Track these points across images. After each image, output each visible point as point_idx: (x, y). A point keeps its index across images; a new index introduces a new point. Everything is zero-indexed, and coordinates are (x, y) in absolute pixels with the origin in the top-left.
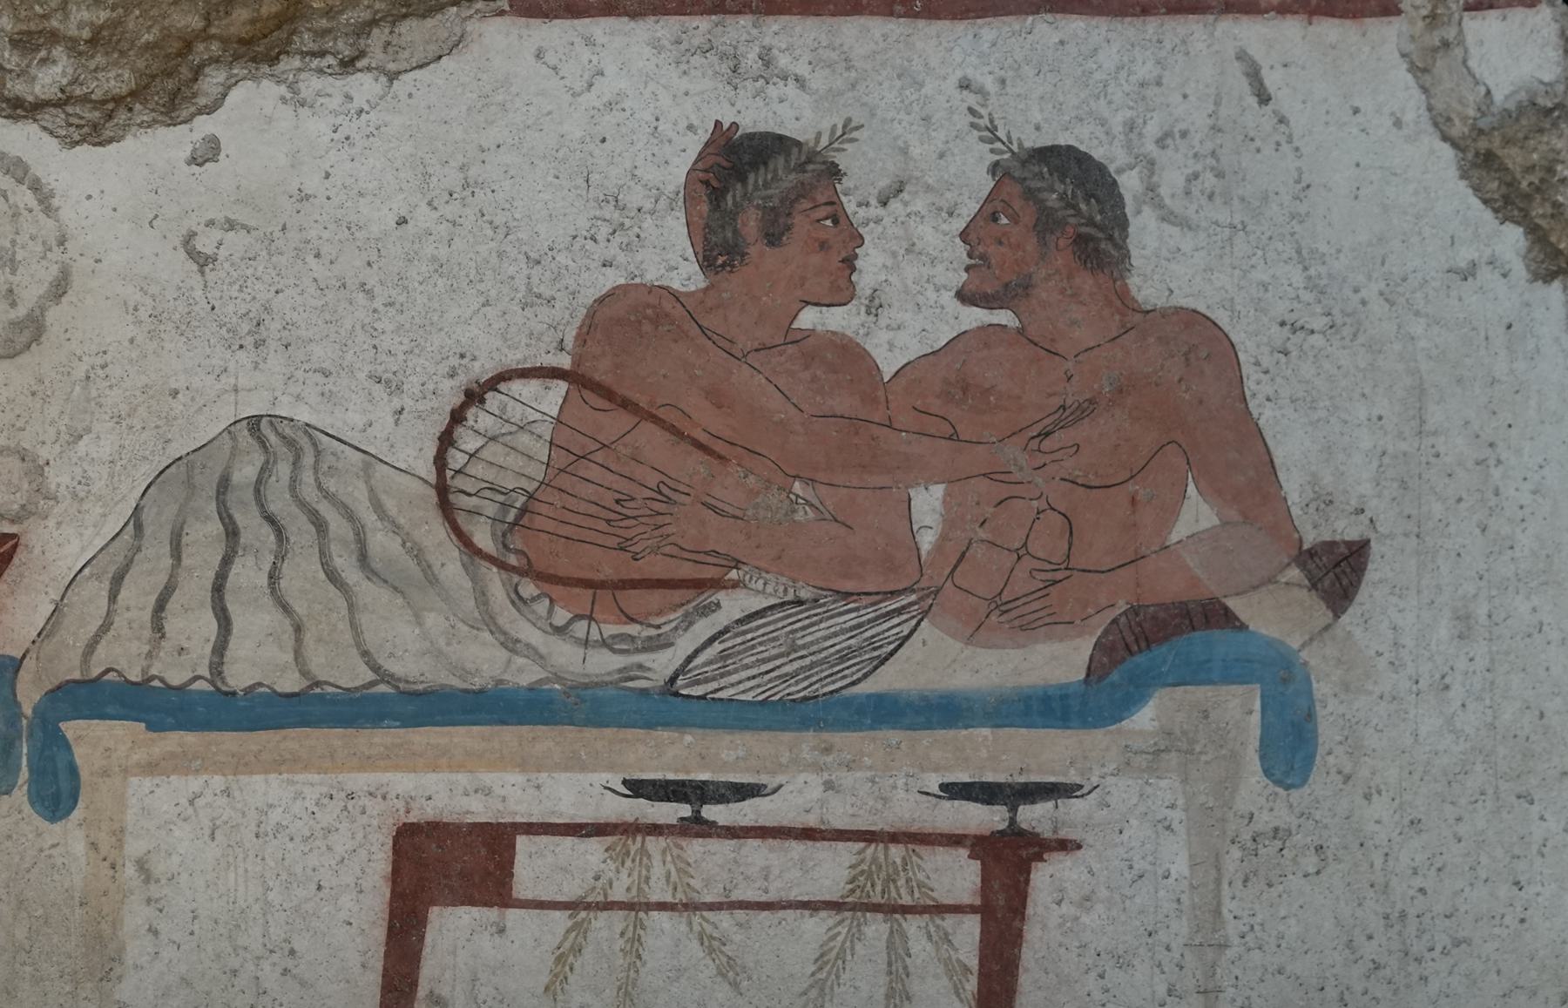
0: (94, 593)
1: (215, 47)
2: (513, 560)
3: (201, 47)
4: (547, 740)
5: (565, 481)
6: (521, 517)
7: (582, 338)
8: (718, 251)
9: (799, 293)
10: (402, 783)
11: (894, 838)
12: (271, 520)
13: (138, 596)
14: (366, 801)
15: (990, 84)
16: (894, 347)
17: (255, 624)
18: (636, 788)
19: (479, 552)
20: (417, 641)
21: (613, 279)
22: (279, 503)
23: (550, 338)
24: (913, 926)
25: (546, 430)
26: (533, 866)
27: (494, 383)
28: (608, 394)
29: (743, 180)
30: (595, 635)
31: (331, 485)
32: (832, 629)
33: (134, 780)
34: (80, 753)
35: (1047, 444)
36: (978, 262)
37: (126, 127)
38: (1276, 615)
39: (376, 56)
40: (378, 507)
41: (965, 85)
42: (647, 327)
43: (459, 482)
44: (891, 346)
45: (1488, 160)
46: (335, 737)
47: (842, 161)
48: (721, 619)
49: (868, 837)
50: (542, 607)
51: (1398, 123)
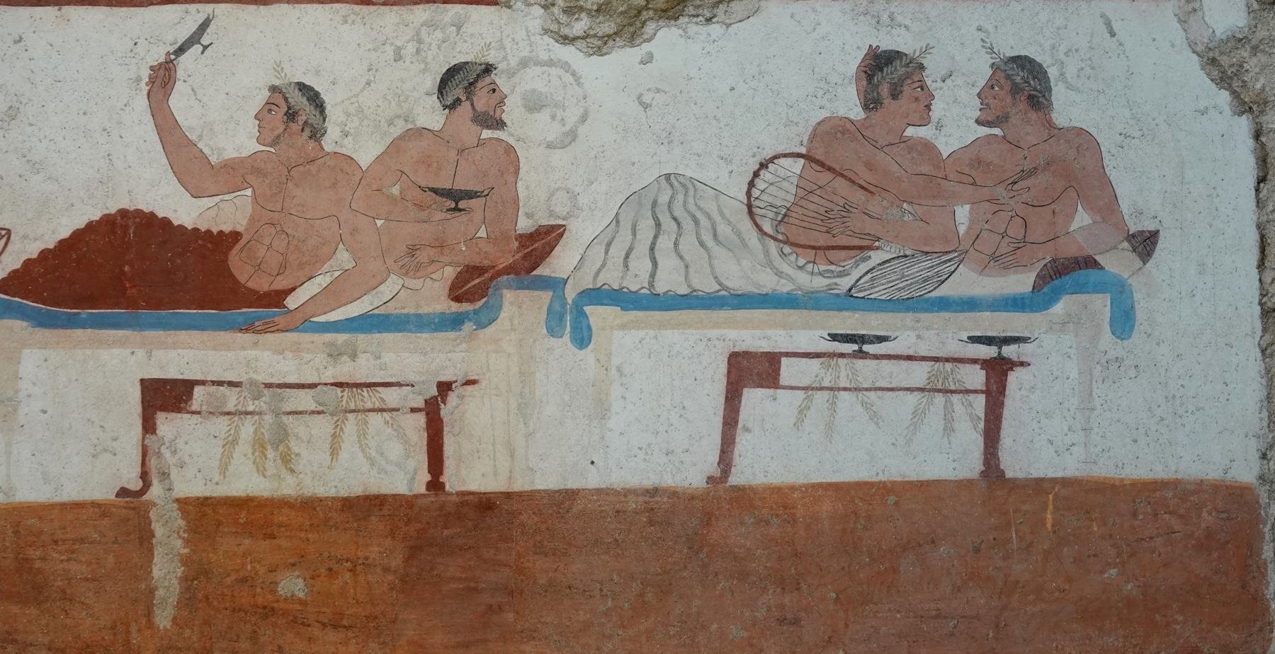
1: (651, 13)
2: (780, 237)
3: (645, 13)
4: (794, 315)
5: (803, 202)
7: (811, 140)
8: (871, 103)
9: (906, 121)
10: (732, 334)
11: (947, 360)
12: (675, 219)
13: (617, 252)
14: (717, 342)
15: (990, 28)
16: (948, 143)
17: (668, 263)
18: (834, 337)
19: (765, 234)
20: (740, 273)
21: (824, 114)
22: (679, 212)
23: (797, 140)
24: (955, 398)
25: (795, 180)
26: (790, 371)
27: (773, 159)
28: (822, 165)
29: (882, 71)
30: (816, 270)
31: (702, 204)
32: (921, 268)
33: (615, 332)
34: (592, 321)
35: (1016, 187)
36: (985, 107)
37: (613, 48)
38: (1118, 262)
39: (721, 15)
40: (721, 213)
41: (979, 29)
42: (839, 135)
43: (757, 203)
44: (947, 144)
45: (1213, 61)
46: (702, 314)
47: (925, 63)
48: (871, 264)
49: (936, 359)
50: (793, 257)
51: (1173, 46)
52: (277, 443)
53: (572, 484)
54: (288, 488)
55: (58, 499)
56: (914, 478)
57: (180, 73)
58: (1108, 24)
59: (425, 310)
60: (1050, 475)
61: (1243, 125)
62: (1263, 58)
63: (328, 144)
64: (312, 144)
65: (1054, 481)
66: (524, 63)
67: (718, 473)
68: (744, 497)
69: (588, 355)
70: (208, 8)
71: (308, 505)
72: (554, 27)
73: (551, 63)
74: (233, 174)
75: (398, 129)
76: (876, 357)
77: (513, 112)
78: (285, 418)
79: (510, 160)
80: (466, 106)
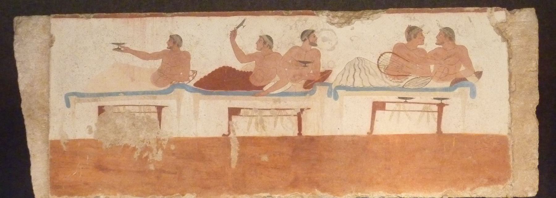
0: (340, 77)
6: (387, 68)
7: (394, 48)
8: (409, 39)
18: (399, 98)
21: (396, 42)
22: (360, 67)
24: (430, 113)
26: (388, 106)
27: (384, 54)
32: (421, 80)
34: (339, 94)
36: (438, 40)
38: (472, 79)
45: (498, 28)
49: (425, 104)
52: (261, 124)
53: (334, 134)
54: (264, 134)
55: (208, 136)
56: (419, 133)
57: (238, 33)
58: (470, 19)
59: (297, 91)
60: (454, 132)
61: (505, 44)
62: (511, 27)
63: (274, 49)
64: (270, 50)
65: (455, 134)
66: (322, 30)
67: (369, 131)
68: (376, 138)
69: (338, 102)
70: (245, 16)
71: (269, 139)
72: (329, 21)
73: (328, 30)
74: (251, 57)
75: (291, 46)
76: (410, 103)
77: (319, 42)
78: (264, 118)
79: (318, 54)
80: (308, 40)
